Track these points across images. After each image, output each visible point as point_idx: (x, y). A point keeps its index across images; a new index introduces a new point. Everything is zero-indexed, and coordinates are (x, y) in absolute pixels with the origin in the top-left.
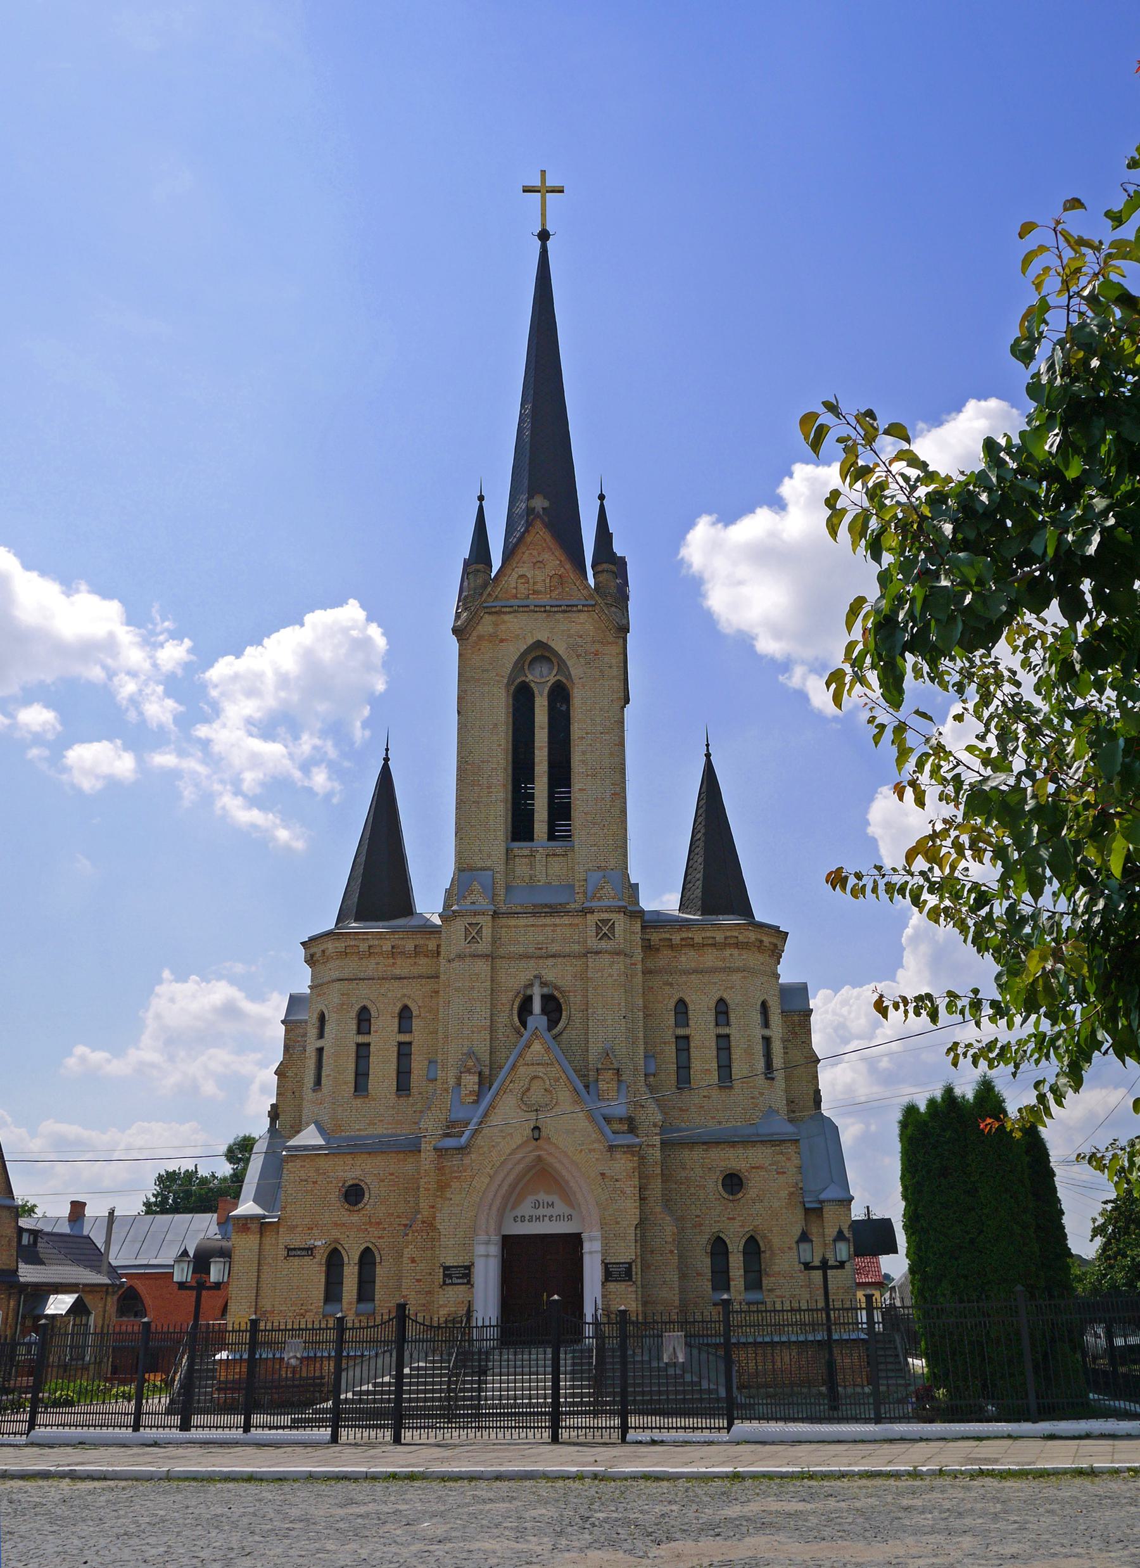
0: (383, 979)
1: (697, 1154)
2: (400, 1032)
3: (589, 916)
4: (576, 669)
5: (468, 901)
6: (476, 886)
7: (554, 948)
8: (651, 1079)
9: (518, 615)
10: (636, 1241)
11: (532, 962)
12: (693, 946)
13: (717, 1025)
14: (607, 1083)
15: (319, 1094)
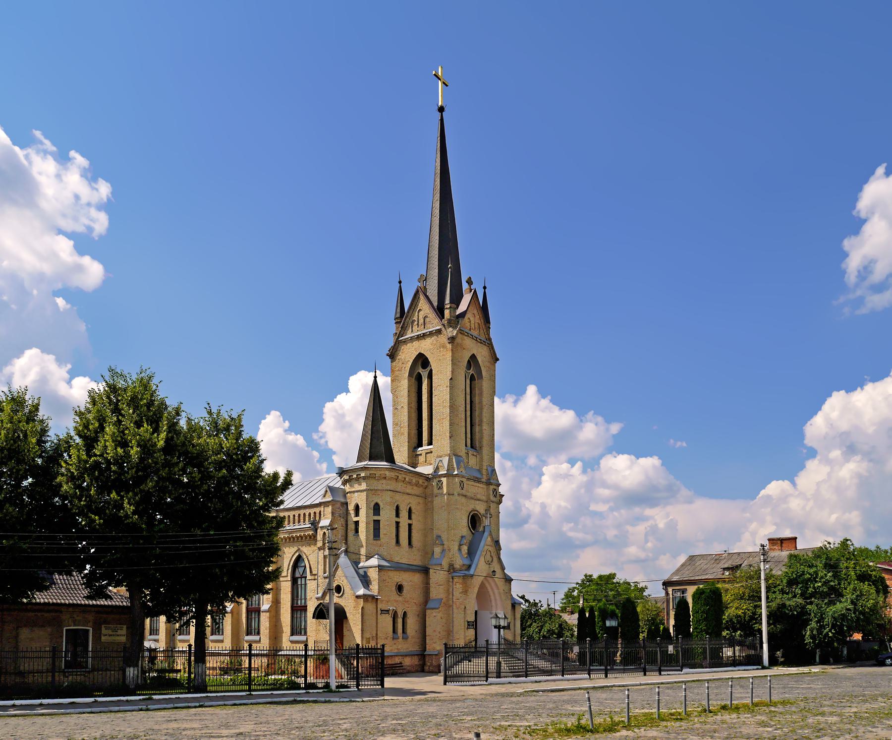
0: (404, 493)
4: (484, 373)
11: (473, 501)
15: (379, 542)
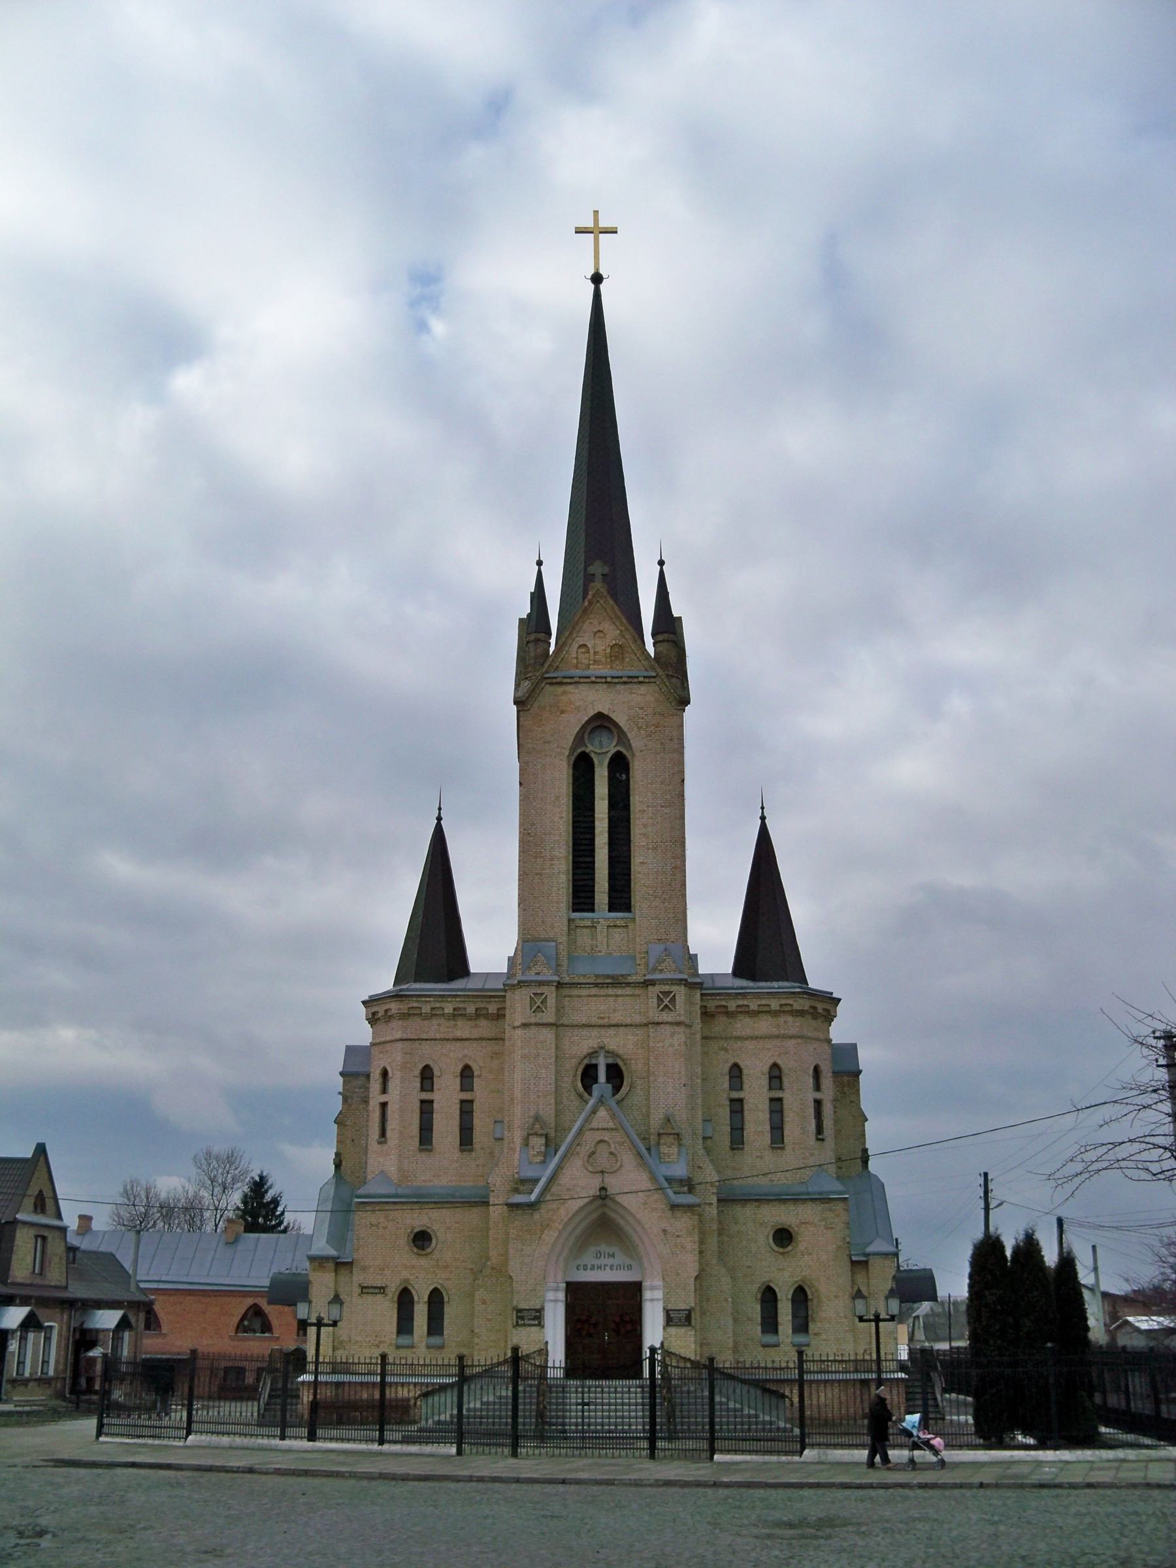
1: (749, 1211)
2: (462, 1090)
3: (650, 987)
4: (638, 741)
5: (533, 972)
6: (540, 957)
7: (617, 1018)
8: (709, 1142)
9: (579, 686)
10: (696, 1290)
11: (595, 1032)
12: (747, 1012)
13: (770, 1089)
14: (668, 1147)
15: (385, 1147)
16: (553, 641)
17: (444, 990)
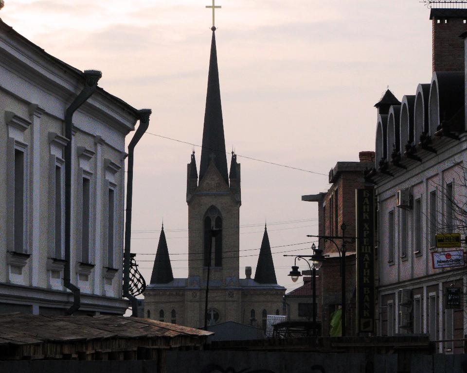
2: (172, 317)
4: (224, 215)
7: (217, 298)
16: (198, 179)
17: (164, 287)
